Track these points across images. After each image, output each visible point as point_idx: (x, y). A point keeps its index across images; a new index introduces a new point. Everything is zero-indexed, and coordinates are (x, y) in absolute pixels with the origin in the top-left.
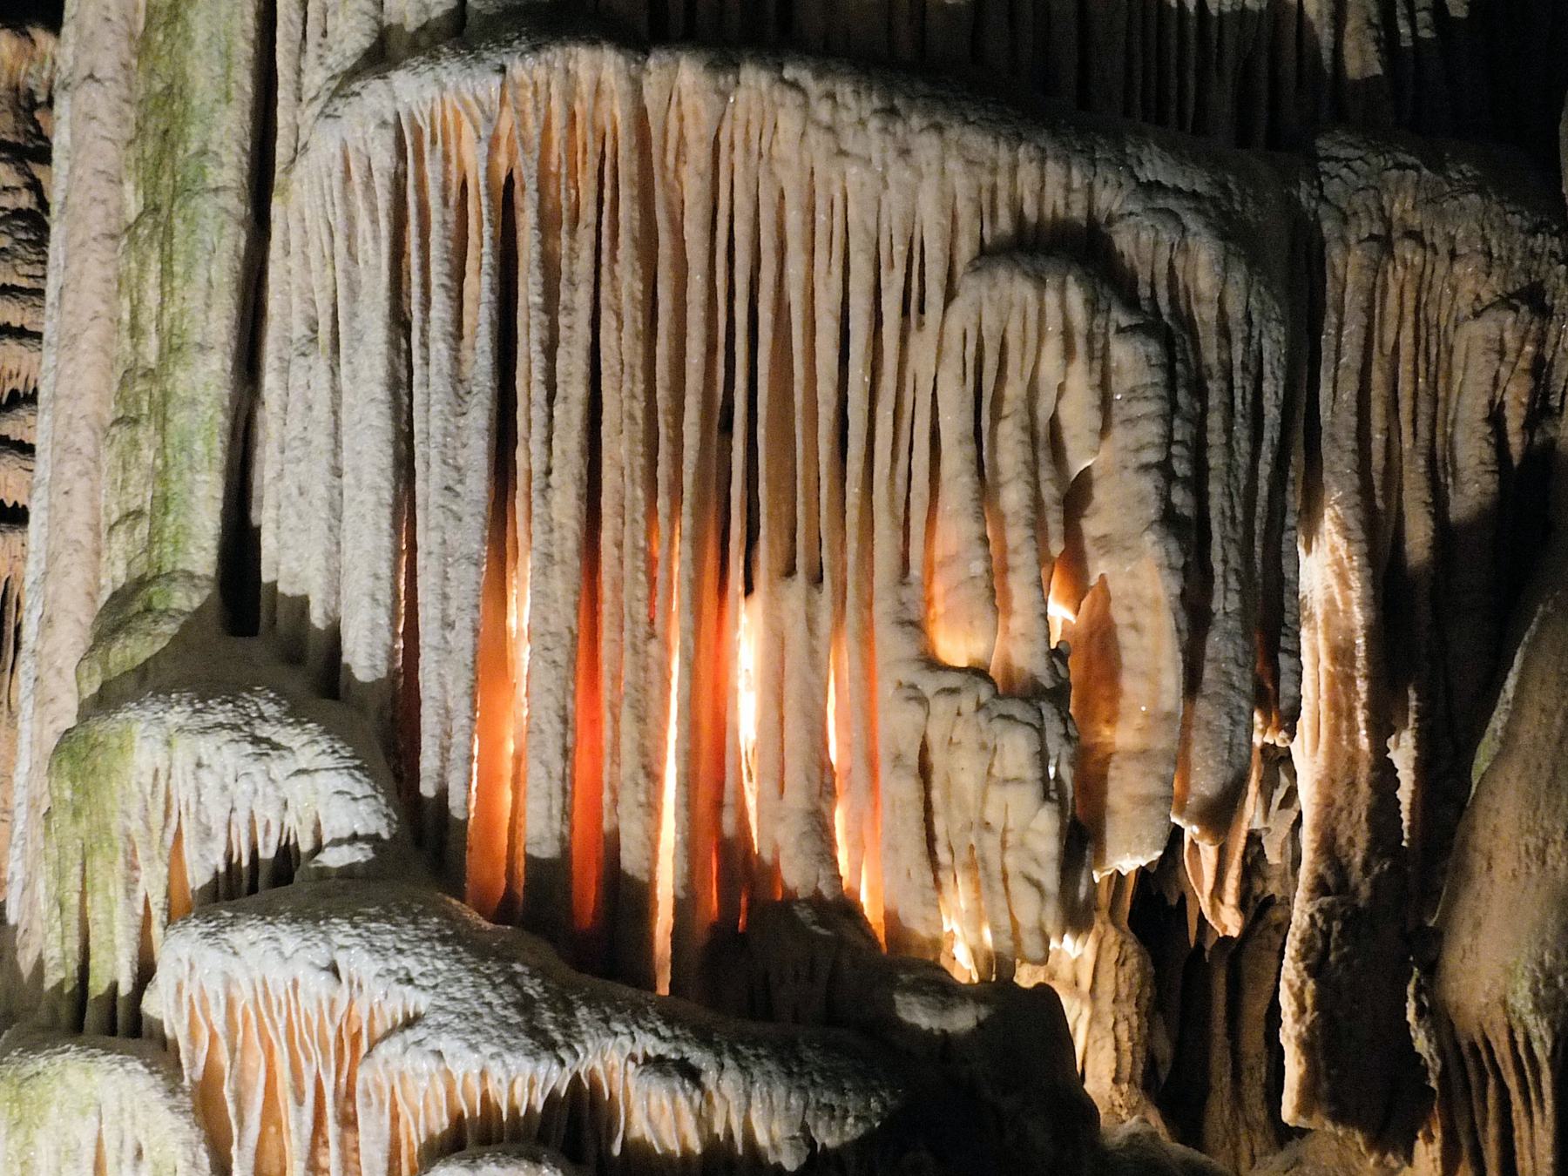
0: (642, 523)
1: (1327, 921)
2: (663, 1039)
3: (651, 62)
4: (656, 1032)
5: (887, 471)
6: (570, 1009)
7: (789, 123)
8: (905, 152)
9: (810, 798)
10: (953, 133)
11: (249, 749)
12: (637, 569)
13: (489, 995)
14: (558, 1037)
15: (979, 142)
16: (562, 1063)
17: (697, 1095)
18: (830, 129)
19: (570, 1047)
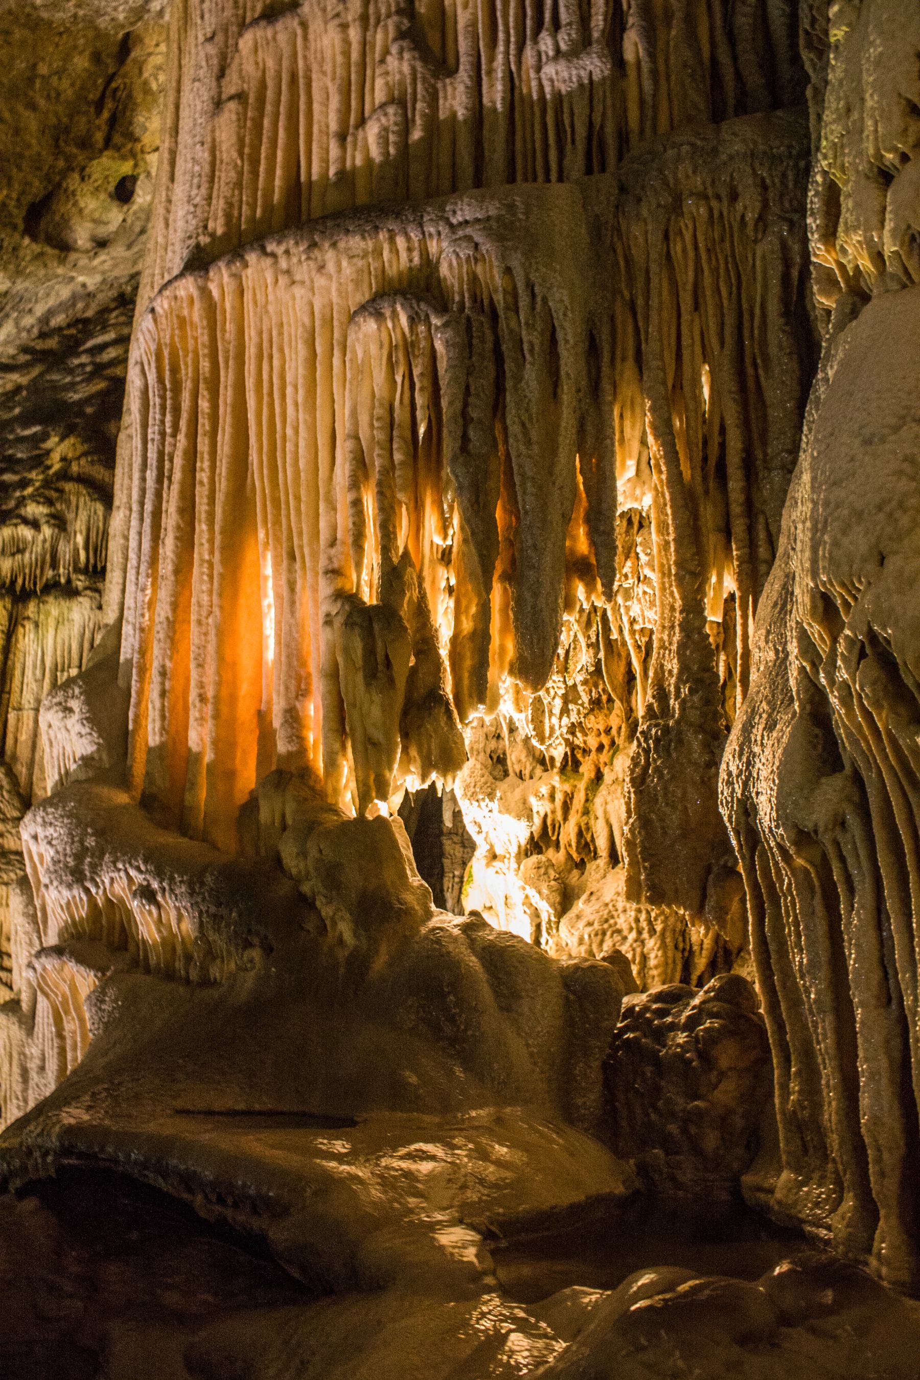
0: (206, 546)
1: (646, 741)
2: (141, 872)
3: (211, 274)
4: (138, 869)
5: (327, 473)
6: (101, 857)
7: (269, 276)
8: (321, 268)
9: (288, 699)
10: (342, 245)
11: (61, 715)
12: (203, 573)
13: (68, 849)
14: (88, 874)
15: (356, 243)
16: (87, 891)
17: (154, 910)
18: (288, 272)
19: (92, 880)
